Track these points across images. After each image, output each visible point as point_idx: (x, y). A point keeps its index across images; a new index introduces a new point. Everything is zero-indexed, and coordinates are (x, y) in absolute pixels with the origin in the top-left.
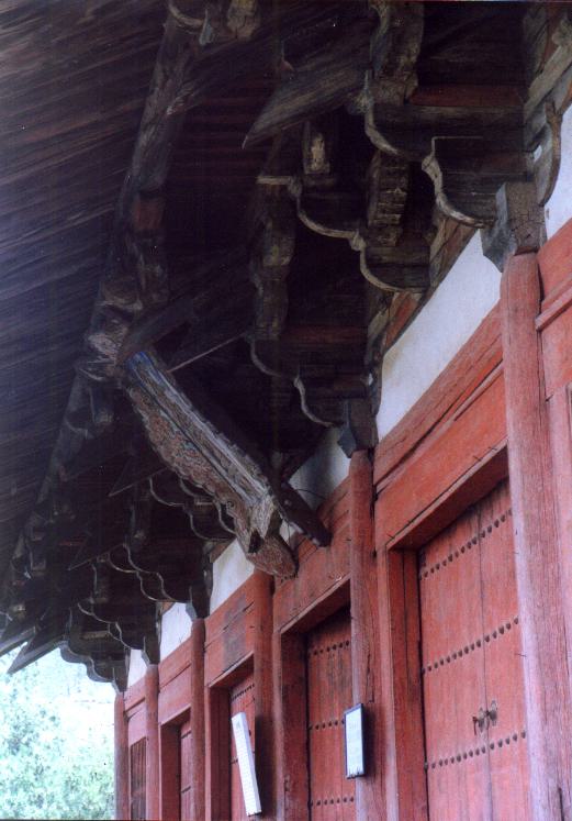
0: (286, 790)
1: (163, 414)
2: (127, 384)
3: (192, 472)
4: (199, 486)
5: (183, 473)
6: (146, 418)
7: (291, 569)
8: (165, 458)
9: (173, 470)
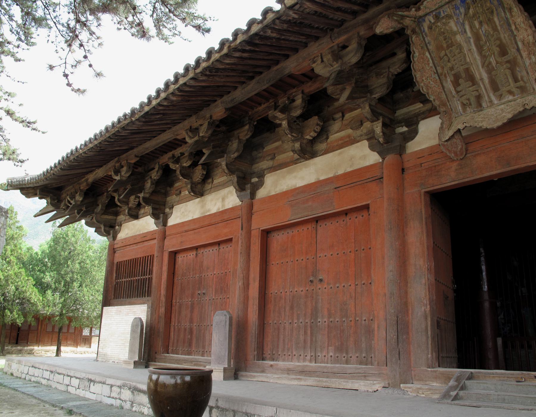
1: (427, 54)
2: (414, 31)
3: (430, 91)
5: (425, 90)
6: (417, 54)
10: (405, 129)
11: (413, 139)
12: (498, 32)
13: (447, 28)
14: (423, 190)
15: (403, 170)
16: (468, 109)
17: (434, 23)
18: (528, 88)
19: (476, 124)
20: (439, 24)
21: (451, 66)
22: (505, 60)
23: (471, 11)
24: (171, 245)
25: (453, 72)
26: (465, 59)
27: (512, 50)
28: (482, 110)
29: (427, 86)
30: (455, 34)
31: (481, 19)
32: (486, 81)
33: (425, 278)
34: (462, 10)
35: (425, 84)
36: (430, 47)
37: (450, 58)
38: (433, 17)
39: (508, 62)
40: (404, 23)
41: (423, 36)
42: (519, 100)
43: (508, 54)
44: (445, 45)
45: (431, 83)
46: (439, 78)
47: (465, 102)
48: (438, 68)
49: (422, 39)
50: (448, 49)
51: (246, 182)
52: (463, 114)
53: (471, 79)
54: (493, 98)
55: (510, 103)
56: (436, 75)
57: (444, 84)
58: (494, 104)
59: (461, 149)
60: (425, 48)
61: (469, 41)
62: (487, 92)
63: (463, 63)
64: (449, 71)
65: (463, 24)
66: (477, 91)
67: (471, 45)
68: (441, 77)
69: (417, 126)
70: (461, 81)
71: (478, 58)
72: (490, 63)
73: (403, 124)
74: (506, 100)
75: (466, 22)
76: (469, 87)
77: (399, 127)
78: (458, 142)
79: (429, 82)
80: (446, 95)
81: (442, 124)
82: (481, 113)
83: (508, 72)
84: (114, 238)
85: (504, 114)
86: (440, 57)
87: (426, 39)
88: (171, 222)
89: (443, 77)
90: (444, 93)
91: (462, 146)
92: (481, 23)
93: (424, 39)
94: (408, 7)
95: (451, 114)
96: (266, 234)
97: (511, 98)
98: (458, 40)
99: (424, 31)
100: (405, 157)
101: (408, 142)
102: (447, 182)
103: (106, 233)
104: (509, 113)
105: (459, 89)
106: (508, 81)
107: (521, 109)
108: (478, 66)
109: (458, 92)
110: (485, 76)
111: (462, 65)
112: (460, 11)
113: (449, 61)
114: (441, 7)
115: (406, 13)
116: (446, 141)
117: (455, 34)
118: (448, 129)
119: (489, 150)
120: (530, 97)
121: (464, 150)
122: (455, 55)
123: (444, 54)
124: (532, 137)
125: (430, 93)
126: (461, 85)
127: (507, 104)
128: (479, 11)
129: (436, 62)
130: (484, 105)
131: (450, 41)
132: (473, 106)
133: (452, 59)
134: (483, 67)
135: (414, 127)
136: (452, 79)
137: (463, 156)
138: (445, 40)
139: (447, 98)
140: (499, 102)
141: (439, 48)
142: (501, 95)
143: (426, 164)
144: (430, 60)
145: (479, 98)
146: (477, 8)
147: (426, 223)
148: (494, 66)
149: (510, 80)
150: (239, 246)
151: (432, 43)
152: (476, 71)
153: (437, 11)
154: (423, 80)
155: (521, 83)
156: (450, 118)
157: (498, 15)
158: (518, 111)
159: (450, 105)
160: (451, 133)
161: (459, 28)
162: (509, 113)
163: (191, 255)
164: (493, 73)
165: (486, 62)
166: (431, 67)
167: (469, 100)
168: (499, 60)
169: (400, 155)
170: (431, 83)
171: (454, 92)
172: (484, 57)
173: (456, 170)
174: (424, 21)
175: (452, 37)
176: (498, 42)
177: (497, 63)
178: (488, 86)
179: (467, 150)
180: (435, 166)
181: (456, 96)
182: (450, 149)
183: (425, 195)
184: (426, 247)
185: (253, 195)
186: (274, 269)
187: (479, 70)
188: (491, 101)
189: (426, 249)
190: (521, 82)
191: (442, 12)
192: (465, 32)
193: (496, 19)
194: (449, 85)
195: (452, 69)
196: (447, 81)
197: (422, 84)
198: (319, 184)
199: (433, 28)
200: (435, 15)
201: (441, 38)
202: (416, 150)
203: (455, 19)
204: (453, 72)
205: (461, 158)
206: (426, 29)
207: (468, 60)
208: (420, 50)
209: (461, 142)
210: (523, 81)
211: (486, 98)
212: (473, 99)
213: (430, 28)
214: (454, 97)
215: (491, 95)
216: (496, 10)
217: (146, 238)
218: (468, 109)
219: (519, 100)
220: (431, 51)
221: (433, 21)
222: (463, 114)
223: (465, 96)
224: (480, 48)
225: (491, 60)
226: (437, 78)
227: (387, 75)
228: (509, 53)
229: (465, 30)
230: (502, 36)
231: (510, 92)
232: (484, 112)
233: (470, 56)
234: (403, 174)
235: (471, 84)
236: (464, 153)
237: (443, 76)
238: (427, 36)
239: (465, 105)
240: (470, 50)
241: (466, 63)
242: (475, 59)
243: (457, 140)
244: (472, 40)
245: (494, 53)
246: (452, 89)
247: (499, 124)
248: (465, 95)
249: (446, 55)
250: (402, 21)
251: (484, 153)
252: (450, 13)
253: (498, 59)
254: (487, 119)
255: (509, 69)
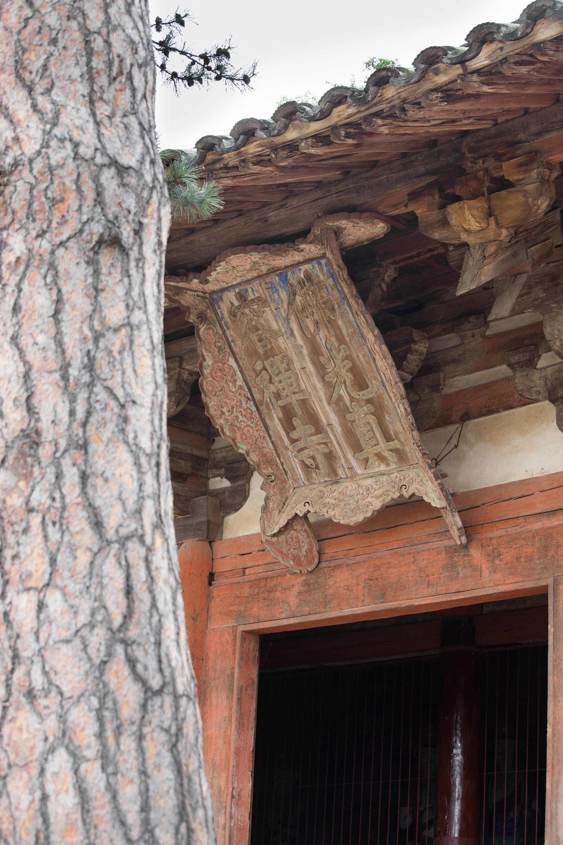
0: (233, 797)
1: (232, 361)
2: (202, 317)
3: (238, 435)
4: (241, 451)
5: (228, 433)
6: (209, 361)
7: (310, 563)
8: (212, 411)
9: (217, 427)
10: (225, 483)
11: (236, 510)
12: (346, 344)
13: (263, 322)
14: (241, 628)
15: (211, 576)
16: (314, 475)
17: (238, 308)
18: (409, 454)
19: (325, 510)
20: (247, 311)
21: (275, 391)
22: (364, 398)
23: (298, 299)
25: (280, 403)
26: (299, 385)
27: (374, 382)
28: (337, 482)
29: (232, 425)
30: (276, 334)
31: (316, 317)
32: (338, 429)
33: (226, 812)
34: (284, 295)
35: (227, 420)
36: (236, 350)
37: (273, 376)
38: (236, 296)
39: (369, 401)
40: (182, 302)
41: (221, 327)
42: (396, 474)
43: (367, 387)
44: (261, 351)
45: (241, 418)
46: (258, 409)
47: (309, 462)
48: (253, 390)
49: (221, 332)
50: (267, 358)
52: (306, 483)
53: (313, 420)
54: (354, 463)
55: (380, 477)
56: (252, 403)
57: (268, 422)
58: (356, 474)
59: (309, 551)
60: (228, 350)
61: (301, 353)
62: (341, 449)
63: (296, 390)
64: (273, 400)
65: (287, 320)
66: (326, 444)
67: (304, 359)
68: (261, 408)
69: (248, 482)
70: (296, 422)
71: (319, 385)
72: (340, 398)
73: (222, 471)
74: (376, 470)
75: (293, 318)
76: (311, 435)
77: (215, 476)
78: (302, 536)
79: (237, 417)
80: (272, 442)
81: (267, 499)
82: (335, 487)
83: (372, 419)
85: (369, 499)
86: (255, 370)
87: (228, 332)
89: (263, 408)
90: (268, 439)
91: (311, 545)
92: (316, 323)
93: (224, 333)
94: (187, 276)
95: (284, 481)
97: (383, 468)
98: (283, 347)
99: (223, 318)
100: (220, 548)
101: (228, 514)
102: (283, 616)
104: (377, 497)
105: (294, 435)
106: (374, 436)
107: (396, 495)
108: (321, 400)
109: (293, 441)
110: (334, 419)
111: (294, 393)
112: (279, 296)
113: (271, 381)
114: (248, 281)
115: (182, 285)
116: (274, 535)
117: (276, 334)
118: (280, 511)
119: (359, 559)
120: (412, 474)
121: (315, 553)
122: (280, 373)
123: (262, 366)
124: (426, 547)
125: (239, 439)
126: (298, 430)
127: (377, 478)
128: (311, 304)
129: (249, 378)
130: (340, 472)
131: (269, 347)
132: (322, 471)
133: (277, 379)
134: (329, 404)
135: (241, 482)
136: (281, 415)
137: (314, 566)
138: (260, 340)
139: (276, 450)
140: (364, 472)
141: (252, 354)
142: (367, 460)
143: (252, 570)
144: (238, 373)
145: (330, 457)
146: (308, 298)
147: (239, 699)
148: (348, 403)
149: (378, 435)
151: (239, 342)
152: (318, 408)
153: (242, 287)
154: (223, 413)
155: (395, 444)
156: (283, 490)
157: (343, 315)
158: (390, 498)
159: (282, 464)
160: (283, 521)
161: (281, 325)
162: (377, 497)
164: (348, 416)
165: (334, 395)
166: (241, 387)
167: (313, 458)
168: (355, 394)
169: (210, 542)
170: (241, 418)
171: (286, 441)
172: (330, 386)
173: (300, 593)
174: (222, 299)
175: (272, 340)
176: (349, 364)
177: (352, 400)
178: (342, 440)
179: (320, 553)
180: (266, 579)
181: (290, 447)
182: (284, 550)
183: (243, 638)
184: (233, 749)
187: (322, 408)
188: (351, 468)
189: (232, 755)
190: (396, 441)
191: (250, 290)
192: (292, 334)
193: (340, 322)
194: (277, 426)
195: (278, 396)
196: (272, 418)
197: (222, 421)
199: (238, 317)
200: (239, 293)
201: (254, 337)
202: (241, 534)
203: (273, 308)
204: (280, 403)
205: (310, 569)
206: (226, 315)
207: (303, 386)
208: (216, 353)
209: (308, 537)
210: (399, 440)
211: (343, 461)
212: (320, 459)
213: (233, 314)
214: (287, 448)
215: (350, 456)
216: (339, 306)
218: (314, 475)
219: (396, 474)
220: (238, 357)
221: (236, 303)
222: (306, 483)
223: (306, 451)
224: (321, 370)
225: (341, 392)
226: (254, 409)
227: (176, 376)
228: (370, 386)
229: (292, 331)
230: (354, 355)
231: (380, 457)
232: (340, 488)
233: (305, 380)
234: (210, 584)
235: (313, 430)
236: (316, 561)
237: (264, 407)
238: (228, 328)
239: (308, 467)
240: (304, 368)
241: (301, 391)
242: (314, 387)
243: (300, 534)
244: (305, 352)
245: (345, 383)
246: (283, 434)
247: (360, 518)
248: (306, 448)
249: (265, 369)
250: (177, 298)
251: (348, 565)
252: (263, 296)
253: (352, 394)
254: (342, 505)
255: (372, 414)
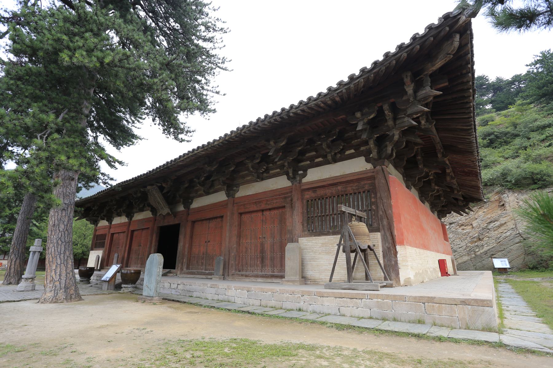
24: (112, 231)
51: (130, 216)
84: (97, 226)
88: (113, 223)
96: (133, 231)
103: (94, 224)
150: (125, 234)
163: (117, 235)
185: (131, 219)
186: (133, 242)
198: (144, 219)
217: (105, 227)
